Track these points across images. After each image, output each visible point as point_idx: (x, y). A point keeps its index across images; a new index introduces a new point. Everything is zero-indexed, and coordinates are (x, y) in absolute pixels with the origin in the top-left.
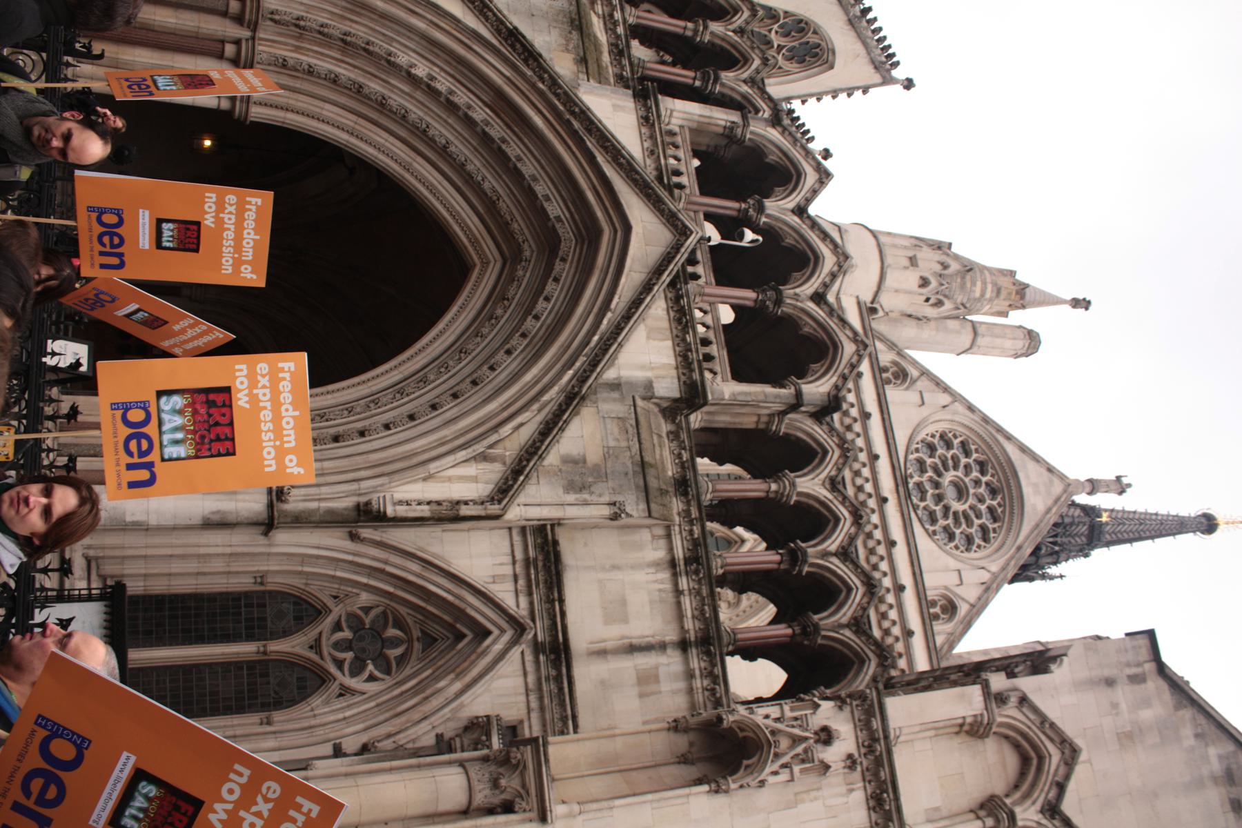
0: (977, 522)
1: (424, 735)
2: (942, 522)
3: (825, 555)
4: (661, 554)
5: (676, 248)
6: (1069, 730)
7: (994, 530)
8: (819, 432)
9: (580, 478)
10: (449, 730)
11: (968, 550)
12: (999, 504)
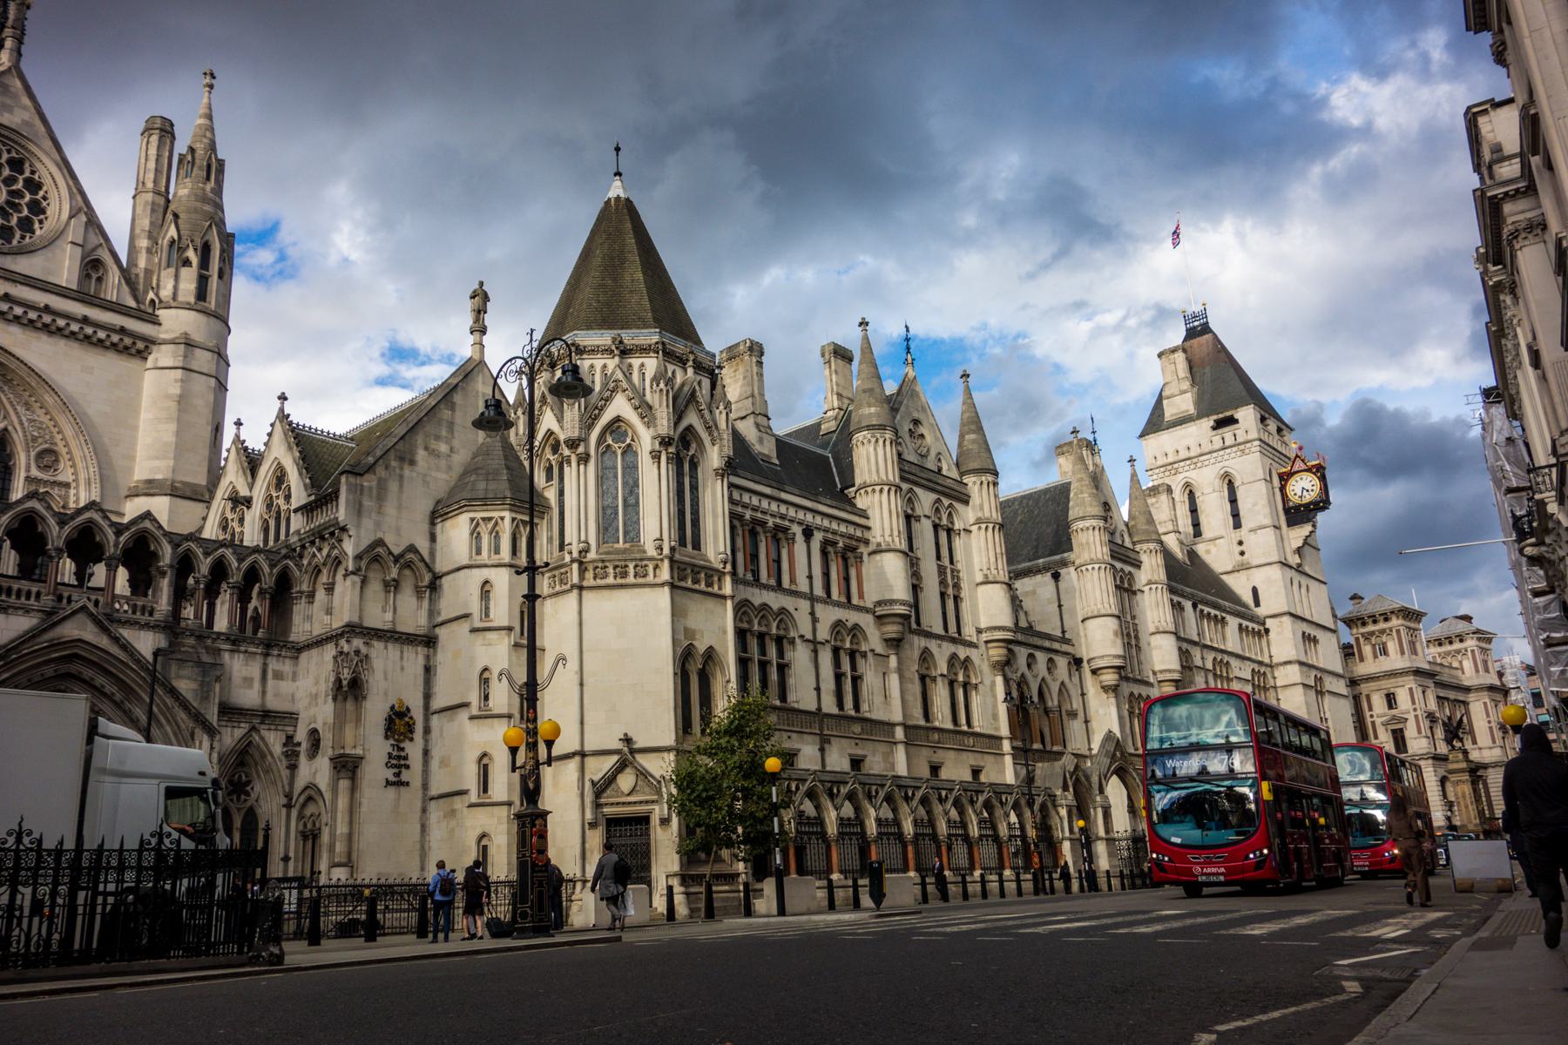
0: (20, 185)
1: (285, 773)
2: (14, 221)
3: (238, 569)
4: (227, 656)
5: (91, 615)
6: (373, 538)
7: (33, 172)
8: (181, 550)
9: (204, 693)
10: (285, 763)
11: (44, 212)
12: (9, 152)
